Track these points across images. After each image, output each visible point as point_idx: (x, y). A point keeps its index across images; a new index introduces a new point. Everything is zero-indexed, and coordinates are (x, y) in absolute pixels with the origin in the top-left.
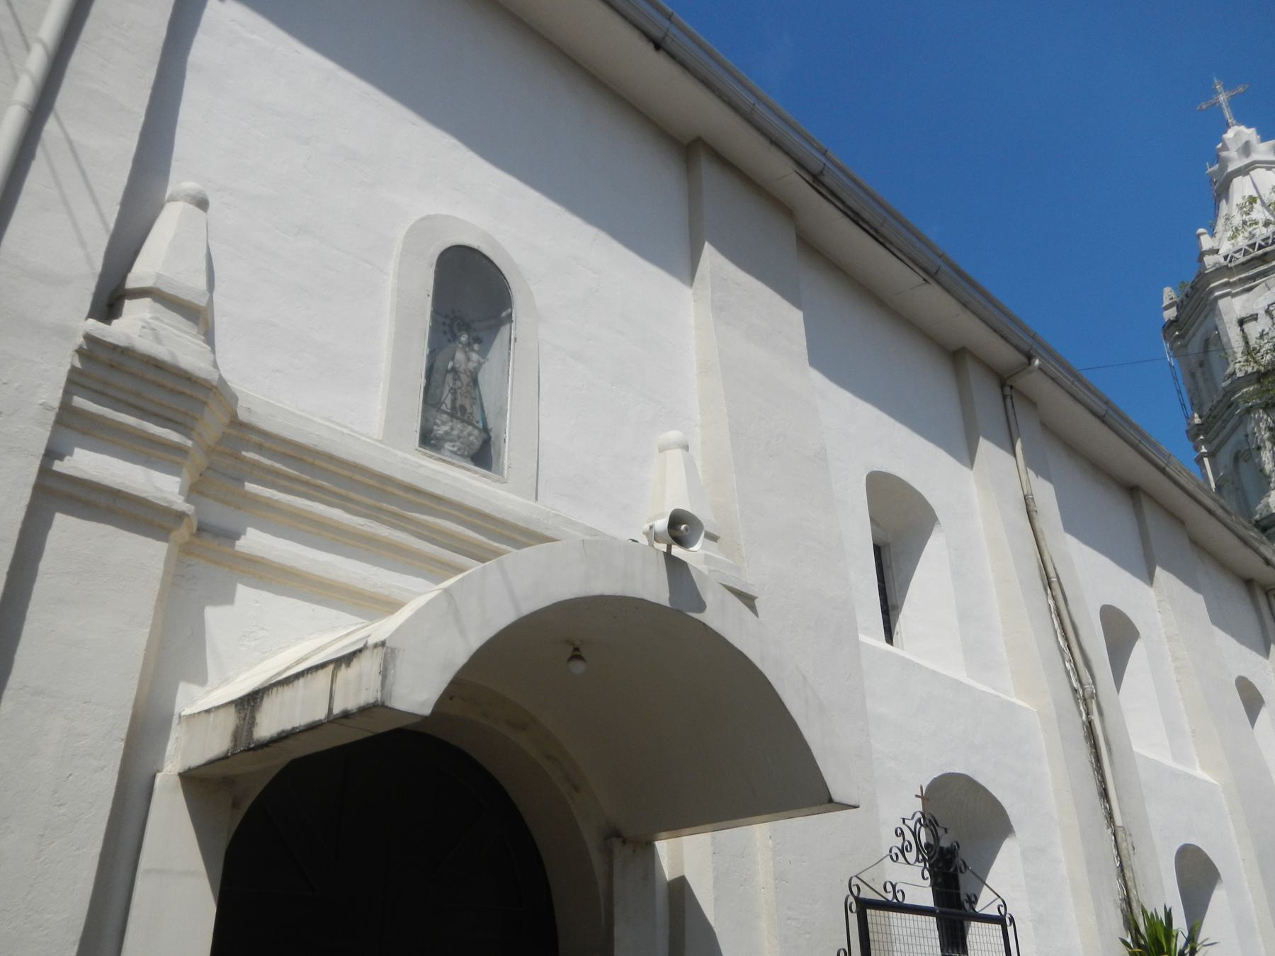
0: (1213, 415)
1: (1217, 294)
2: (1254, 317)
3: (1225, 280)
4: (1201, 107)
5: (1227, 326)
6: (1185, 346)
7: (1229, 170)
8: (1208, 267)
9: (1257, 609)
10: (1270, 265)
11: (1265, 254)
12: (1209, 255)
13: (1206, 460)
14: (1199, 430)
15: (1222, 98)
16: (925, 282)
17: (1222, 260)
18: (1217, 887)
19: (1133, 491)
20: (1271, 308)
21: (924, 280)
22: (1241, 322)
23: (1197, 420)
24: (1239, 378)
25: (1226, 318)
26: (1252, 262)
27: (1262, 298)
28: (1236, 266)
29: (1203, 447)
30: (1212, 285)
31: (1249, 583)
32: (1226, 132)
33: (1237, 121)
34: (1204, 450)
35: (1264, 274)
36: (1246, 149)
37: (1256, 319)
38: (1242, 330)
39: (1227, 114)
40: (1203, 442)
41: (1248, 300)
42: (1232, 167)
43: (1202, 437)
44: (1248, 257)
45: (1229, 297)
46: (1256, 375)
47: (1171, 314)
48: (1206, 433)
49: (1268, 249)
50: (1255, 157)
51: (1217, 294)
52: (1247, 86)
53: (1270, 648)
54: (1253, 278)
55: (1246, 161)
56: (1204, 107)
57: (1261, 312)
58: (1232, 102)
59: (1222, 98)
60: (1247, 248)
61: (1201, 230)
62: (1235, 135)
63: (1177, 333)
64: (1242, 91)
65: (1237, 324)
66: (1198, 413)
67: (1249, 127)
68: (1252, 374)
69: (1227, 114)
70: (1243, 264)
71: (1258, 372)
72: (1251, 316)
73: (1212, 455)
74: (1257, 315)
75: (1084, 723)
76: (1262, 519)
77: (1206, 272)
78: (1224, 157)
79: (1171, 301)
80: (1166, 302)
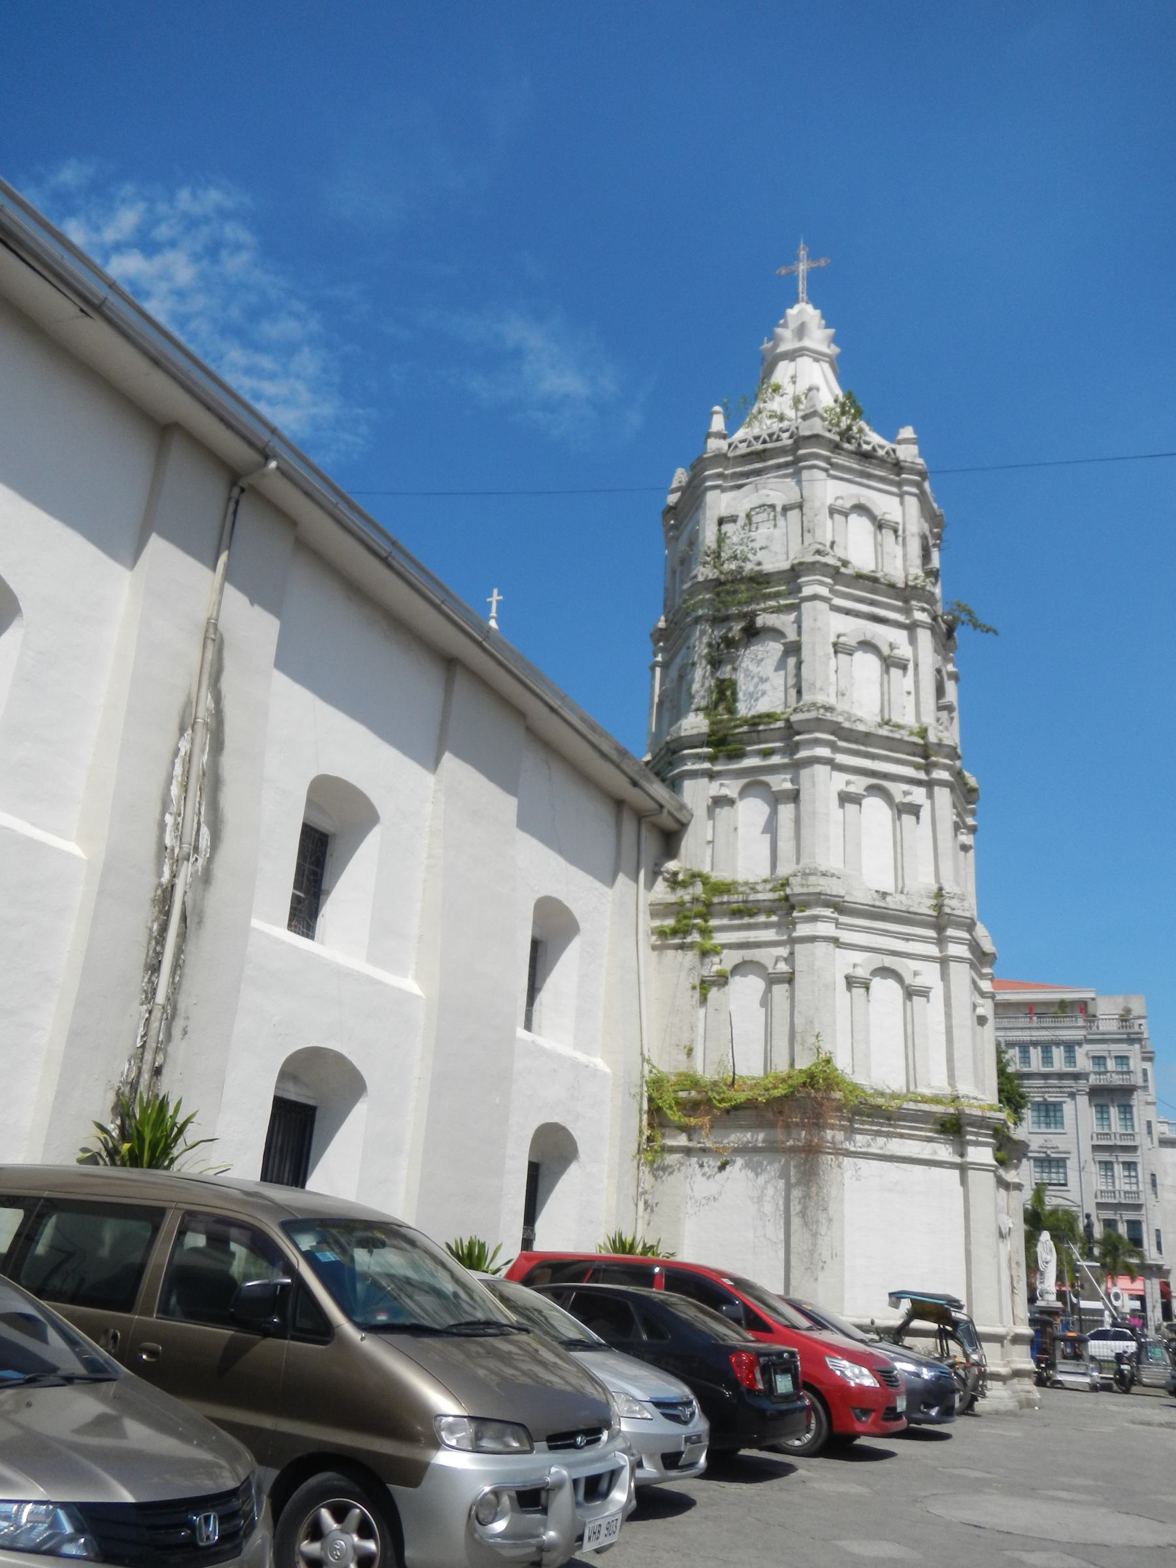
0: (675, 620)
1: (709, 484)
3: (720, 470)
4: (780, 272)
5: (708, 522)
6: (676, 539)
7: (780, 350)
8: (709, 451)
9: (619, 835)
11: (764, 451)
12: (716, 437)
13: (658, 670)
14: (661, 635)
15: (802, 267)
16: (81, 314)
17: (725, 447)
18: (361, 1100)
19: (450, 663)
20: (753, 513)
21: (82, 310)
22: (721, 522)
23: (662, 624)
24: (698, 582)
25: (709, 513)
27: (748, 499)
28: (735, 457)
29: (660, 655)
30: (707, 473)
31: (619, 804)
32: (791, 307)
33: (809, 298)
34: (659, 658)
35: (758, 473)
36: (801, 332)
38: (719, 530)
39: (802, 286)
40: (662, 650)
41: (734, 499)
42: (783, 348)
43: (661, 644)
44: (749, 450)
45: (718, 491)
46: (714, 583)
47: (673, 499)
48: (666, 640)
49: (769, 446)
50: (807, 343)
51: (709, 484)
52: (829, 261)
53: (618, 875)
55: (797, 345)
56: (783, 271)
57: (742, 515)
58: (812, 275)
59: (802, 267)
60: (752, 439)
61: (717, 408)
62: (799, 313)
63: (672, 522)
65: (717, 522)
66: (665, 617)
67: (816, 307)
68: (712, 580)
69: (802, 286)
70: (743, 456)
71: (717, 580)
72: (732, 516)
73: (665, 666)
75: (160, 885)
76: (673, 741)
77: (705, 456)
79: (679, 485)
80: (675, 485)
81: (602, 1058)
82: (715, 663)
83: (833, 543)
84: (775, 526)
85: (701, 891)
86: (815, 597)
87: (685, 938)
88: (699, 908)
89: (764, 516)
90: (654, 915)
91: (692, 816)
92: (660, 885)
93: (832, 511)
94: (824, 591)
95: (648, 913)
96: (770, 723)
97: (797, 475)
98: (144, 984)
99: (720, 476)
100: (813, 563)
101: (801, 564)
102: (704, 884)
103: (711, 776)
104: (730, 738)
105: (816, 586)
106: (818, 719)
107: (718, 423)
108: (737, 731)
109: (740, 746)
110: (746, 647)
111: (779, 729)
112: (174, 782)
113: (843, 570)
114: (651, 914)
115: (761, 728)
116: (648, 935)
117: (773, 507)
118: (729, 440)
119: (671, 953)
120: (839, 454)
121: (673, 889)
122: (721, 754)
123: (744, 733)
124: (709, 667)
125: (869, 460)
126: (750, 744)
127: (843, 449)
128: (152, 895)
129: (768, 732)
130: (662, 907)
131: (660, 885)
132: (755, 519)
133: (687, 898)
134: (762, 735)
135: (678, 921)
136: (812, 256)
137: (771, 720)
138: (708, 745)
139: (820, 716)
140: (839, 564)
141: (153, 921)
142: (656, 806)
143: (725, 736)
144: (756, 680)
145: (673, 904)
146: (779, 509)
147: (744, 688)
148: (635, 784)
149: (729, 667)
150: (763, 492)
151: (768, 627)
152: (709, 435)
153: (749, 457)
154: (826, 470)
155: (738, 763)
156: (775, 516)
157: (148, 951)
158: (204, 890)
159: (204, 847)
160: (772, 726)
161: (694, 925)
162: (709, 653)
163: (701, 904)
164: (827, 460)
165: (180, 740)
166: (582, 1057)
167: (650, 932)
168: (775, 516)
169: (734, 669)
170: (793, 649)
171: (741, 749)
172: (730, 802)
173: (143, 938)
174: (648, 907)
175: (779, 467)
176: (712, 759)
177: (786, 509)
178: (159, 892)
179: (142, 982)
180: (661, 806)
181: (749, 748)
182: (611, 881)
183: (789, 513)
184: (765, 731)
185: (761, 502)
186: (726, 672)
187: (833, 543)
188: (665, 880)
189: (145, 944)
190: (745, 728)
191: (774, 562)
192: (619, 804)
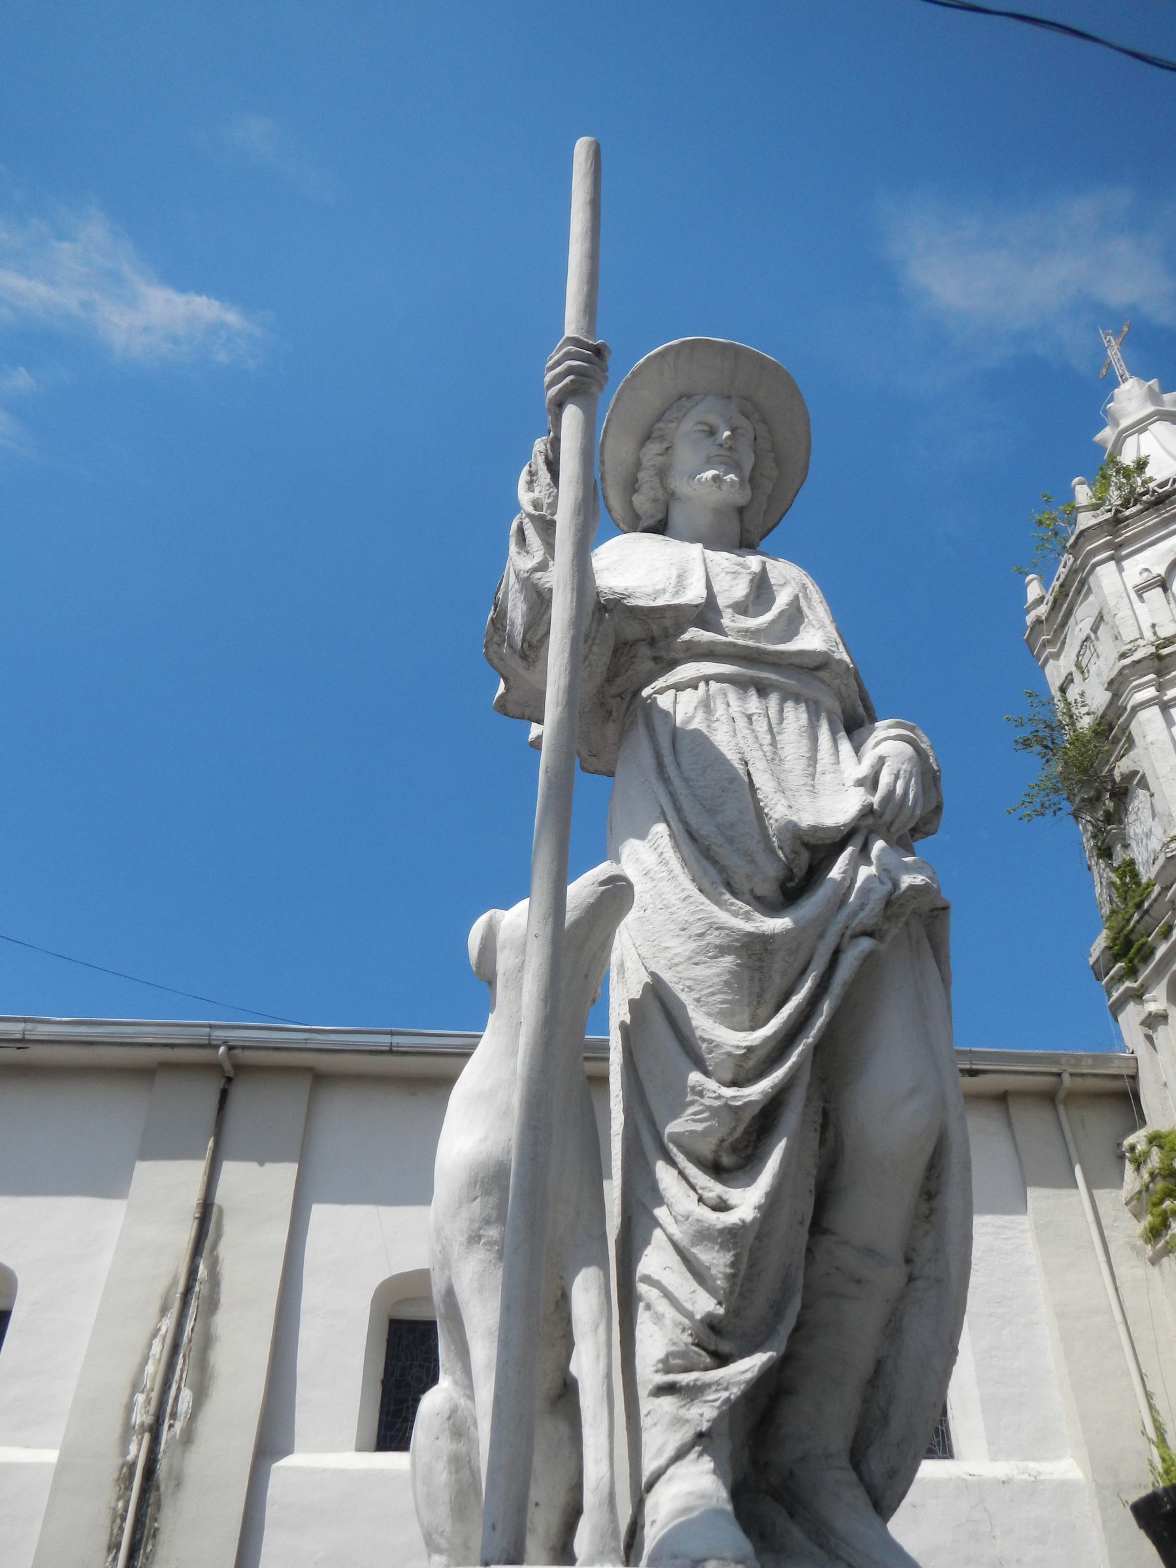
2: (1069, 679)
10: (1069, 598)
12: (1034, 609)
26: (1058, 604)
35: (1069, 613)
37: (1072, 681)
39: (1119, 368)
45: (1051, 661)
50: (1124, 423)
54: (1064, 624)
56: (1104, 371)
57: (1074, 669)
64: (1127, 329)
70: (1053, 608)
72: (1066, 678)
74: (1071, 674)
78: (1098, 441)
81: (1072, 1456)
82: (1106, 853)
83: (1154, 626)
84: (1098, 655)
85: (1158, 1160)
86: (1136, 709)
87: (1166, 1235)
88: (1160, 1185)
89: (1088, 651)
90: (1137, 1216)
91: (1137, 1060)
92: (1129, 1168)
93: (1141, 591)
94: (1150, 692)
95: (1130, 1215)
96: (1150, 893)
97: (1090, 589)
98: (107, 1564)
99: (1044, 646)
100: (1120, 673)
101: (1111, 683)
102: (1161, 1147)
103: (1138, 996)
104: (1133, 937)
105: (1135, 695)
106: (1168, 859)
107: (1034, 590)
108: (1132, 923)
109: (1140, 942)
110: (1126, 810)
111: (1159, 894)
112: (150, 1362)
113: (1165, 652)
114: (1135, 1216)
115: (1146, 905)
116: (1134, 1247)
117: (1087, 638)
118: (1045, 602)
119: (1165, 1260)
120: (1127, 526)
121: (1138, 1169)
122: (1136, 961)
123: (1138, 922)
124: (1101, 861)
125: (1167, 502)
126: (1149, 936)
127: (1127, 518)
128: (116, 1475)
129: (1155, 905)
130: (1135, 1202)
131: (1129, 1168)
132: (1084, 664)
133: (1146, 1177)
134: (1150, 912)
135: (1152, 1215)
136: (1116, 334)
137: (1149, 890)
138: (1117, 958)
139: (1169, 855)
140: (1153, 649)
141: (118, 1499)
142: (1052, 1079)
143: (1127, 936)
144: (1144, 841)
145: (1140, 1192)
146: (1093, 636)
147: (1140, 860)
148: (973, 1073)
149: (1119, 847)
150: (1077, 629)
151: (1127, 775)
152: (1028, 611)
153: (1056, 608)
154: (1111, 558)
155: (1153, 961)
156: (1094, 646)
157: (112, 1530)
158: (184, 1452)
159: (185, 1409)
160: (1153, 896)
161: (1165, 1212)
162: (1096, 845)
163: (1159, 1178)
164: (1107, 546)
165: (161, 1320)
166: (1001, 1469)
167: (1140, 1242)
168: (1094, 646)
169: (1126, 846)
170: (1144, 784)
171: (1143, 945)
172: (1163, 1018)
173: (105, 1519)
174: (1127, 1208)
175: (1079, 592)
176: (1132, 972)
177: (1095, 629)
178: (125, 1470)
179: (106, 1562)
180: (1059, 1075)
181: (1150, 939)
182: (1019, 1206)
183: (1099, 633)
184: (1151, 905)
185: (1079, 643)
186: (1119, 855)
187: (1154, 626)
188: (1131, 1161)
189: (108, 1524)
190: (1136, 917)
191: (1099, 699)
192: (1002, 1098)
